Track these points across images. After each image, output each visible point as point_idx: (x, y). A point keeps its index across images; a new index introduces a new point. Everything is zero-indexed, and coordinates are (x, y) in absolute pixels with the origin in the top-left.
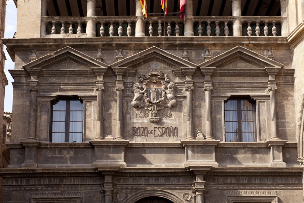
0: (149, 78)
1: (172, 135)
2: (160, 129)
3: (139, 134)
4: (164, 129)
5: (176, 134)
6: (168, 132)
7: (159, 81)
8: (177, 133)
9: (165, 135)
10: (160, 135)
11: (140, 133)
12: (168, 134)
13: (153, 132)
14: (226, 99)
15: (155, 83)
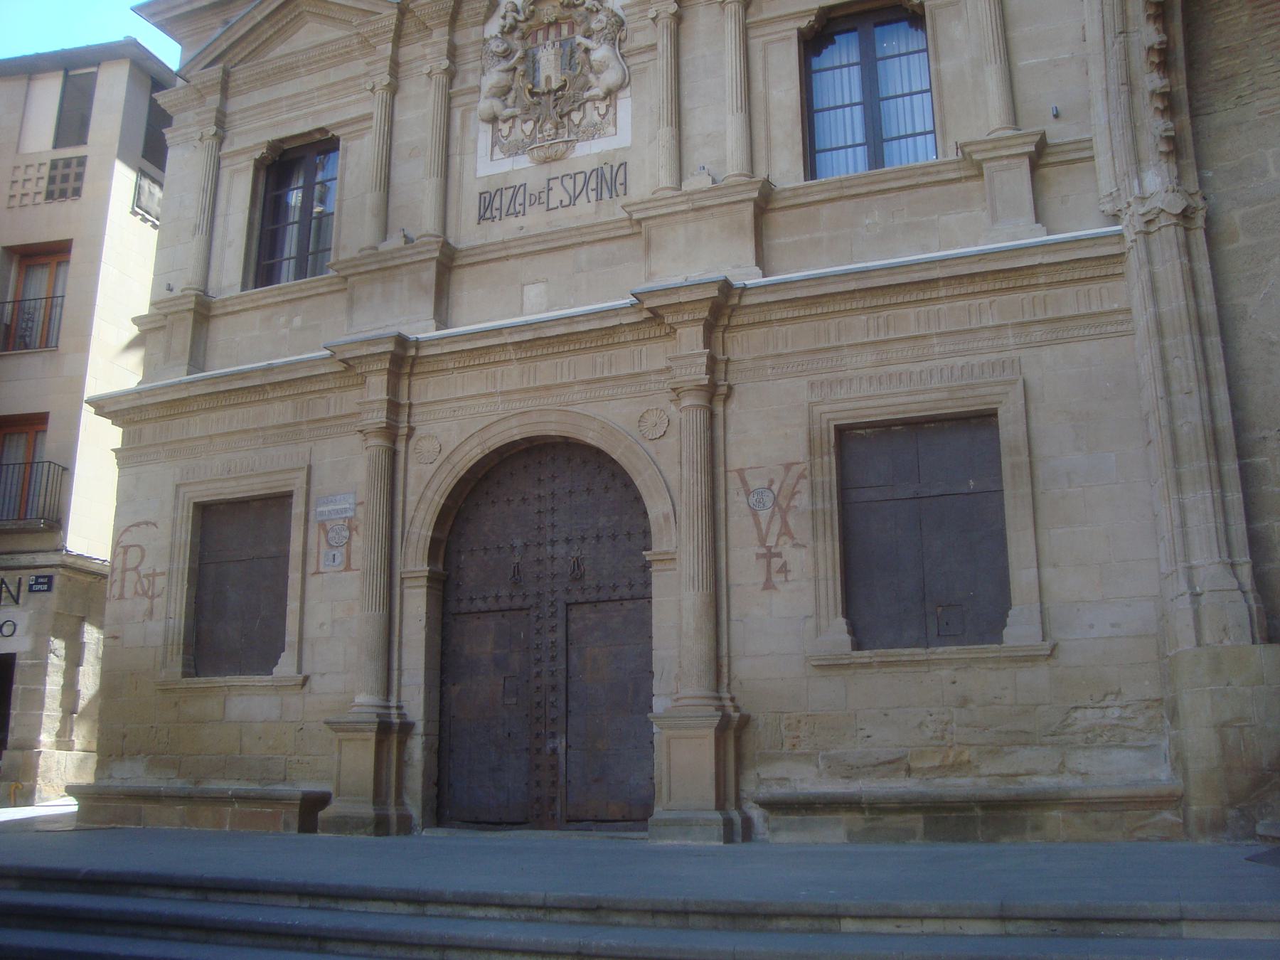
0: (533, 12)
1: (606, 195)
2: (569, 183)
3: (496, 213)
4: (580, 179)
5: (620, 189)
6: (594, 187)
7: (567, 14)
8: (625, 184)
9: (583, 198)
10: (566, 202)
11: (500, 209)
12: (593, 195)
13: (544, 196)
14: (804, 24)
15: (550, 24)
